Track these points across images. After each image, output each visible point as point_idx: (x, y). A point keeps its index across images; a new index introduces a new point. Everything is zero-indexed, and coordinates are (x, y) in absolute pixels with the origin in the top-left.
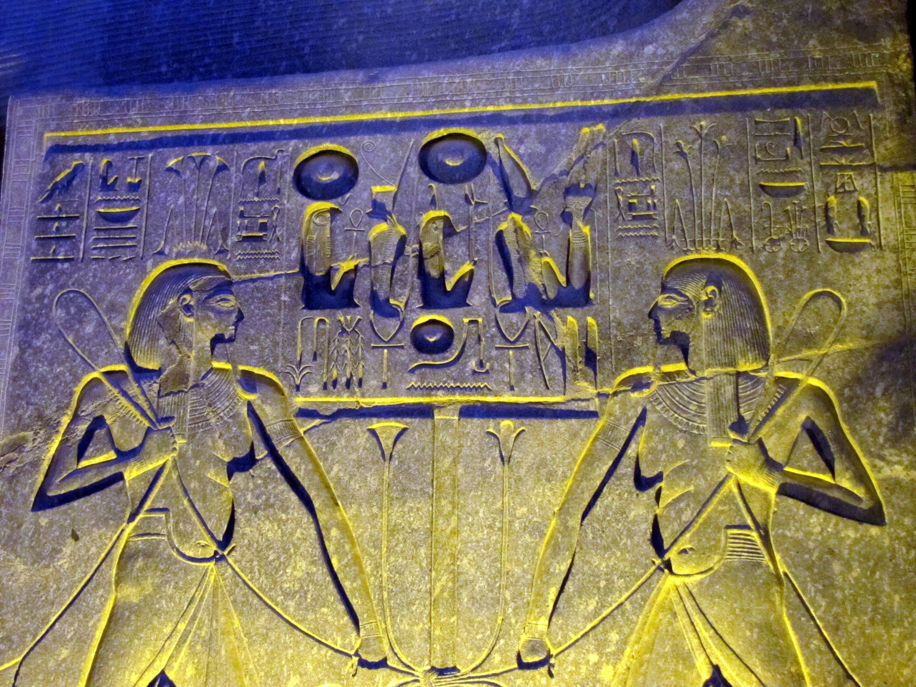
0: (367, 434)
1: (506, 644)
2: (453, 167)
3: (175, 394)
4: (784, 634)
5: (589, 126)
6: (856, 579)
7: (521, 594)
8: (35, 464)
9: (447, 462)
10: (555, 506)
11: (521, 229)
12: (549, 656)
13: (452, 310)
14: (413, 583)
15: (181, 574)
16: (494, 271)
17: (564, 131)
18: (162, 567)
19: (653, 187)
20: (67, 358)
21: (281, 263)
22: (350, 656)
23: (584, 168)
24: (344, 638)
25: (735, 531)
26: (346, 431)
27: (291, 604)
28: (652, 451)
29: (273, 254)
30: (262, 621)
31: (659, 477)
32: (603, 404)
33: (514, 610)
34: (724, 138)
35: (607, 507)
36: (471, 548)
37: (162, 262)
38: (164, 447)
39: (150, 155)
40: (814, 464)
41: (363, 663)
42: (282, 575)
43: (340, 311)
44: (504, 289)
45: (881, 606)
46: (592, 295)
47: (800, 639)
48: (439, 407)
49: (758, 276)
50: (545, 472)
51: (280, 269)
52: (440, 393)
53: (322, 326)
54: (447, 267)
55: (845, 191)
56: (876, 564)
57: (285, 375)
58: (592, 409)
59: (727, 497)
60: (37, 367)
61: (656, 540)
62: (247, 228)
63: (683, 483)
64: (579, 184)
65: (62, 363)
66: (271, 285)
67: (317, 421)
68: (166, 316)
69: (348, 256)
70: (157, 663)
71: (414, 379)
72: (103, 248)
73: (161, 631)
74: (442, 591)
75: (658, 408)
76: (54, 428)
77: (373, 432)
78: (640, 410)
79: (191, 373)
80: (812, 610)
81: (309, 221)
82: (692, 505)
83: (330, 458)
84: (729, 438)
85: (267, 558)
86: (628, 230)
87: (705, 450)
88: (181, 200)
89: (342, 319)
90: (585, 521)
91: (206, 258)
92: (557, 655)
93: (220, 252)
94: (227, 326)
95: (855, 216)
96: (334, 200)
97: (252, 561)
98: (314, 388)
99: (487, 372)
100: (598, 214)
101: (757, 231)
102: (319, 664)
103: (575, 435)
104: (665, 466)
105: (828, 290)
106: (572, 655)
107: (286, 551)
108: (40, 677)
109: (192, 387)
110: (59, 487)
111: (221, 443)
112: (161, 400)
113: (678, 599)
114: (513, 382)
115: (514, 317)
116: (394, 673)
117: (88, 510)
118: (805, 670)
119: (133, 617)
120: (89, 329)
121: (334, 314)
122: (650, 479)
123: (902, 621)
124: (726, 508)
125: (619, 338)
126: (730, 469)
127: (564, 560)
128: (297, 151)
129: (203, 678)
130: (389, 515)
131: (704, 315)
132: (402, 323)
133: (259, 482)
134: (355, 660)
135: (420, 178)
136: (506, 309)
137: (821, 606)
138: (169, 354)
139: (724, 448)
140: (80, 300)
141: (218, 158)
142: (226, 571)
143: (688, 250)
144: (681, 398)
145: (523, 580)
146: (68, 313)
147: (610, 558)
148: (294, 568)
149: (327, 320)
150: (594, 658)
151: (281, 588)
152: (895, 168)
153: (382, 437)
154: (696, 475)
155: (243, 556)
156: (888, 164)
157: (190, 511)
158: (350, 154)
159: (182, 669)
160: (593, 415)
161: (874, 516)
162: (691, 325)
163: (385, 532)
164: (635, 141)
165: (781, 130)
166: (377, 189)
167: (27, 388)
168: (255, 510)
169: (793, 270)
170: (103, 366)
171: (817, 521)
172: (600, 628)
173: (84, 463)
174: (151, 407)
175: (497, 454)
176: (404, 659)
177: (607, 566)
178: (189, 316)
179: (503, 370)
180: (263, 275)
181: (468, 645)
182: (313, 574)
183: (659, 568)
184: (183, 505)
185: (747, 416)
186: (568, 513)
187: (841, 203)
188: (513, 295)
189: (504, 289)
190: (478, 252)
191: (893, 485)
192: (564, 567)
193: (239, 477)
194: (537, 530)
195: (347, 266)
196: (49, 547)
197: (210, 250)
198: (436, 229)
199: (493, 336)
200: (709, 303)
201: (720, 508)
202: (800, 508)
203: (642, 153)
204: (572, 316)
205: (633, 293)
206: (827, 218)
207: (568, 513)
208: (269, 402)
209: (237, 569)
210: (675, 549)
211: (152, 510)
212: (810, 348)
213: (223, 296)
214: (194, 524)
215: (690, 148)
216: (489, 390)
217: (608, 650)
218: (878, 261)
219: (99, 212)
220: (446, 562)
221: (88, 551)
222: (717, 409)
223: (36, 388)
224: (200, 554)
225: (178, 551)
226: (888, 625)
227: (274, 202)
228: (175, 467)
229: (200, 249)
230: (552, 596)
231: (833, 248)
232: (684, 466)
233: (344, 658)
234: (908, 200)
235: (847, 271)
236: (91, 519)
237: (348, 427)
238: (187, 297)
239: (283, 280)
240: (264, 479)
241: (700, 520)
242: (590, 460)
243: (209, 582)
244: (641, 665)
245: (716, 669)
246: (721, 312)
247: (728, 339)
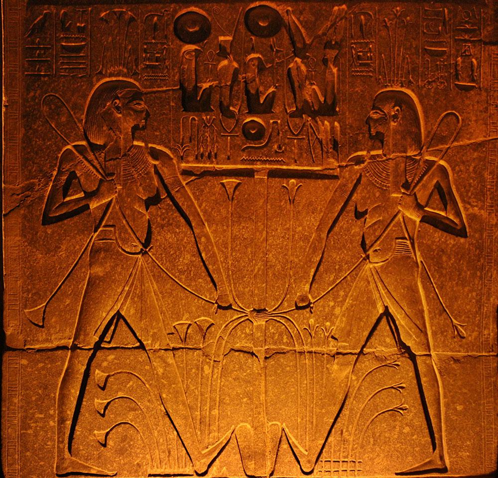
0: (220, 185)
1: (290, 297)
2: (263, 26)
3: (115, 159)
4: (418, 292)
5: (338, 6)
6: (452, 264)
7: (297, 272)
8: (41, 198)
9: (261, 202)
10: (315, 226)
11: (300, 67)
12: (310, 303)
13: (264, 115)
14: (244, 266)
15: (124, 261)
16: (287, 93)
17: (324, 8)
18: (114, 257)
19: (371, 46)
20: (53, 136)
21: (169, 83)
22: (213, 303)
23: (335, 32)
25: (400, 240)
26: (209, 184)
27: (183, 277)
28: (363, 198)
29: (165, 76)
30: (168, 286)
31: (366, 212)
32: (341, 171)
34: (408, 18)
35: (342, 227)
36: (273, 248)
37: (102, 78)
38: (111, 190)
39: (90, 9)
40: (439, 206)
41: (220, 307)
43: (203, 113)
44: (292, 104)
45: (461, 277)
46: (337, 109)
47: (426, 293)
48: (256, 171)
49: (421, 102)
50: (311, 207)
51: (168, 87)
52: (258, 163)
53: (194, 122)
54: (261, 89)
55: (466, 55)
56: (461, 257)
57: (174, 151)
58: (336, 174)
59: (397, 223)
60: (36, 142)
61: (363, 244)
62: (149, 59)
63: (377, 215)
64: (331, 42)
65: (49, 140)
66: (164, 95)
67: (193, 178)
68: (105, 113)
69: (207, 79)
70: (115, 307)
71: (245, 155)
72: (66, 68)
73: (116, 291)
74: (258, 271)
75: (367, 175)
76: (50, 178)
77: (223, 184)
78: (358, 175)
79: (122, 147)
80: (432, 279)
81: (183, 56)
82: (381, 227)
83: (201, 198)
84: (401, 192)
85: (169, 253)
86: (358, 71)
87: (389, 198)
88: (110, 39)
89: (205, 118)
90: (330, 235)
91: (126, 77)
92: (314, 302)
93: (133, 74)
94: (141, 120)
95: (469, 69)
96: (198, 44)
97: (161, 254)
98: (191, 159)
99: (283, 152)
100: (342, 60)
101: (421, 76)
102: (199, 307)
103: (327, 188)
104: (369, 206)
105: (454, 112)
106: (321, 302)
107: (179, 249)
108: (57, 313)
109: (123, 156)
110: (55, 211)
111: (141, 189)
112: (107, 163)
113: (371, 275)
114: (296, 158)
115: (297, 120)
116: (236, 312)
117: (73, 225)
118: (425, 308)
119: (101, 283)
120: (63, 119)
121: (201, 115)
122: (362, 212)
123: (470, 283)
124: (396, 229)
125: (351, 135)
126: (400, 208)
127: (318, 255)
128: (176, 11)
129: (139, 315)
130: (232, 230)
131: (393, 124)
132: (237, 121)
133: (164, 211)
134: (216, 305)
135: (246, 33)
136: (292, 115)
137: (436, 277)
138: (109, 136)
139: (397, 197)
140: (56, 101)
141: (130, 13)
142: (148, 260)
143: (387, 85)
144: (379, 169)
145: (299, 265)
146: (50, 109)
147: (341, 254)
148: (184, 258)
149: (196, 119)
150: (332, 304)
151: (177, 269)
152: (491, 43)
153: (228, 187)
154: (384, 211)
156: (488, 41)
157: (127, 227)
158: (206, 15)
159: (128, 310)
160: (336, 177)
161: (462, 233)
162: (386, 129)
163: (230, 240)
164: (362, 17)
165: (437, 16)
166: (221, 38)
167: (32, 154)
168: (162, 226)
170: (73, 142)
171: (438, 235)
172: (335, 289)
173: (68, 199)
174: (101, 167)
175: (288, 198)
176: (240, 305)
177: (340, 258)
178: (119, 113)
179: (292, 151)
180: (160, 89)
181: (272, 298)
182: (194, 261)
183: (364, 259)
184: (123, 223)
185: (410, 180)
186: (321, 230)
187: (463, 62)
188: (296, 107)
189: (292, 104)
190: (278, 80)
191: (472, 218)
192: (318, 259)
193: (153, 209)
194: (306, 239)
195: (206, 86)
196: (53, 245)
197: (128, 73)
198: (254, 65)
199: (286, 131)
200: (395, 117)
201: (394, 229)
202: (430, 229)
203: (366, 25)
204: (328, 121)
205: (359, 109)
206: (456, 70)
207: (321, 230)
208: (166, 165)
209: (154, 259)
210: (372, 249)
211: (106, 226)
212: (442, 144)
213: (137, 101)
214: (129, 234)
215: (391, 23)
216: (284, 162)
217: (339, 300)
218: (478, 96)
219: (62, 45)
220: (260, 256)
221: (75, 248)
222: (396, 177)
223: (37, 153)
224: (133, 250)
225: (122, 248)
226: (463, 286)
227: (164, 44)
228: (117, 202)
229: (123, 72)
230: (312, 274)
231: (458, 88)
232: (378, 206)
233: (211, 304)
234: (495, 62)
235: (463, 101)
236: (75, 230)
237: (209, 181)
238: (117, 101)
239: (171, 93)
240: (166, 210)
241: (384, 235)
242: (333, 202)
243: (138, 266)
244: (352, 307)
245: (386, 308)
246: (401, 122)
247: (404, 138)
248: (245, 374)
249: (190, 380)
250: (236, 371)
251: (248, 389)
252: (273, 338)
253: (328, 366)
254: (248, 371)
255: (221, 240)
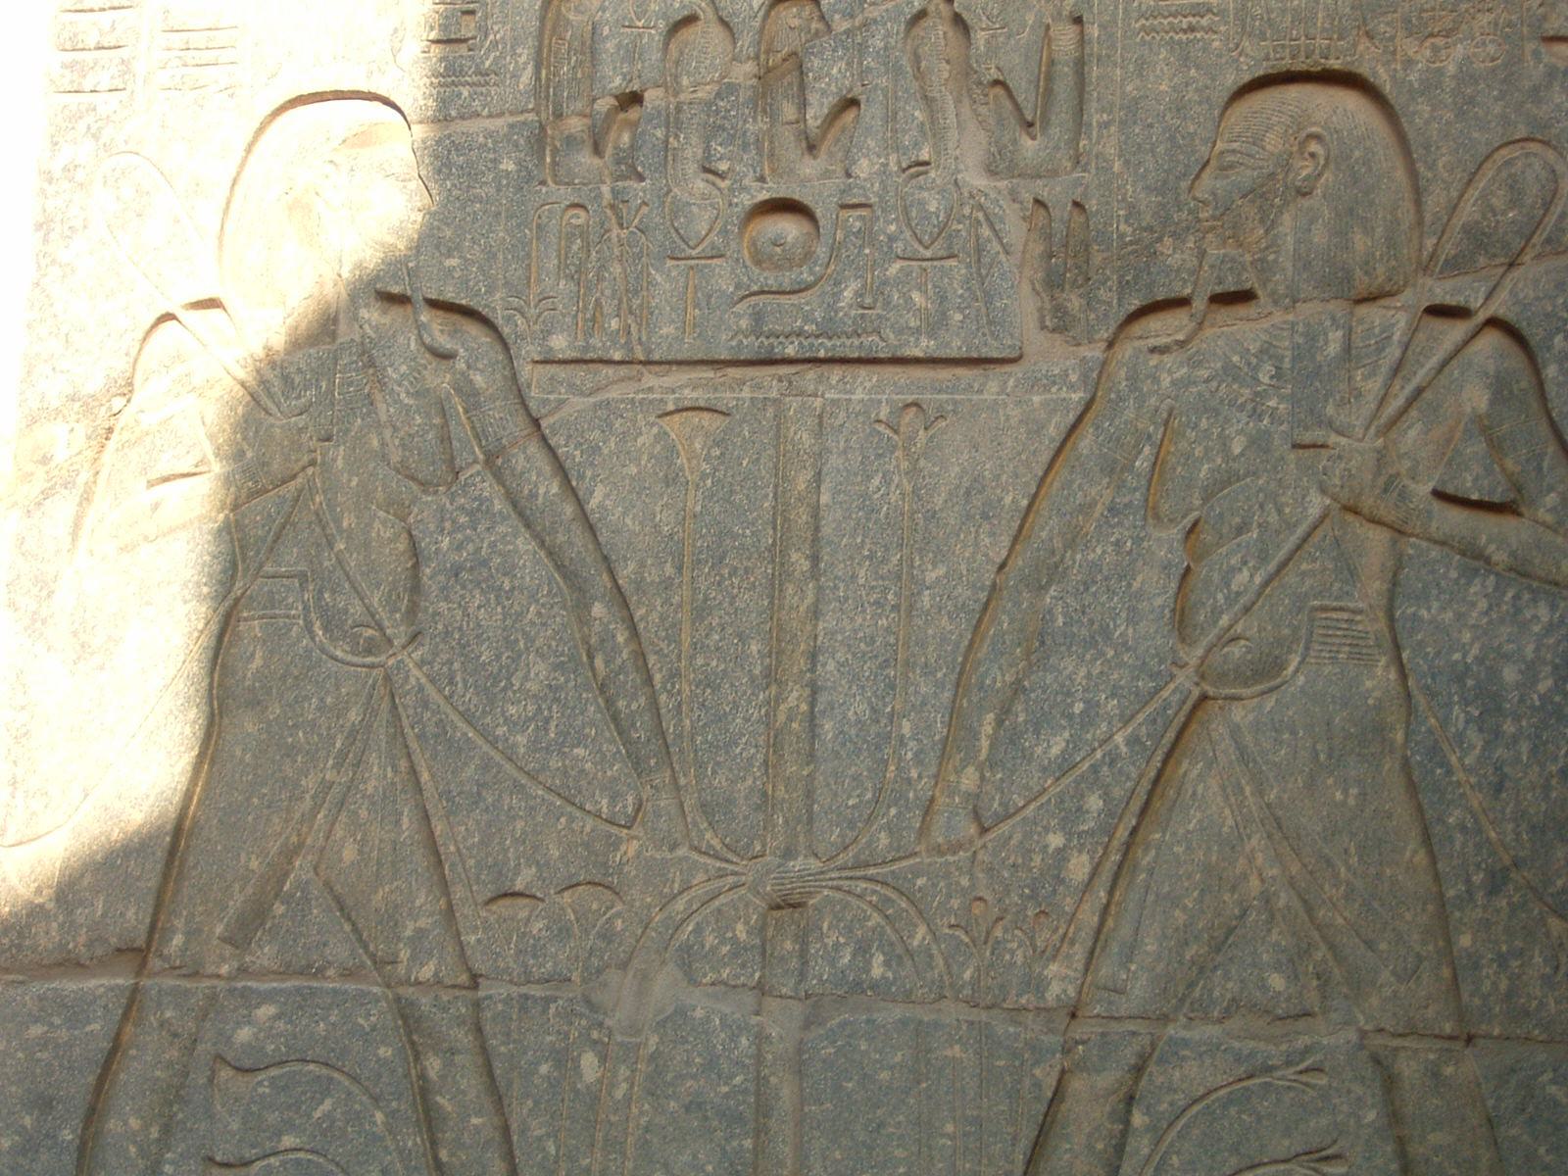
24: (614, 798)
26: (617, 424)
33: (916, 755)
42: (505, 689)
74: (790, 719)
107: (510, 644)
151: (503, 713)
155: (436, 654)
169: (1471, 101)
240: (471, 513)
248: (725, 1089)
249: (530, 1103)
250: (694, 1077)
251: (735, 1143)
252: (832, 963)
253: (1037, 1072)
254: (738, 1080)
255: (654, 616)
